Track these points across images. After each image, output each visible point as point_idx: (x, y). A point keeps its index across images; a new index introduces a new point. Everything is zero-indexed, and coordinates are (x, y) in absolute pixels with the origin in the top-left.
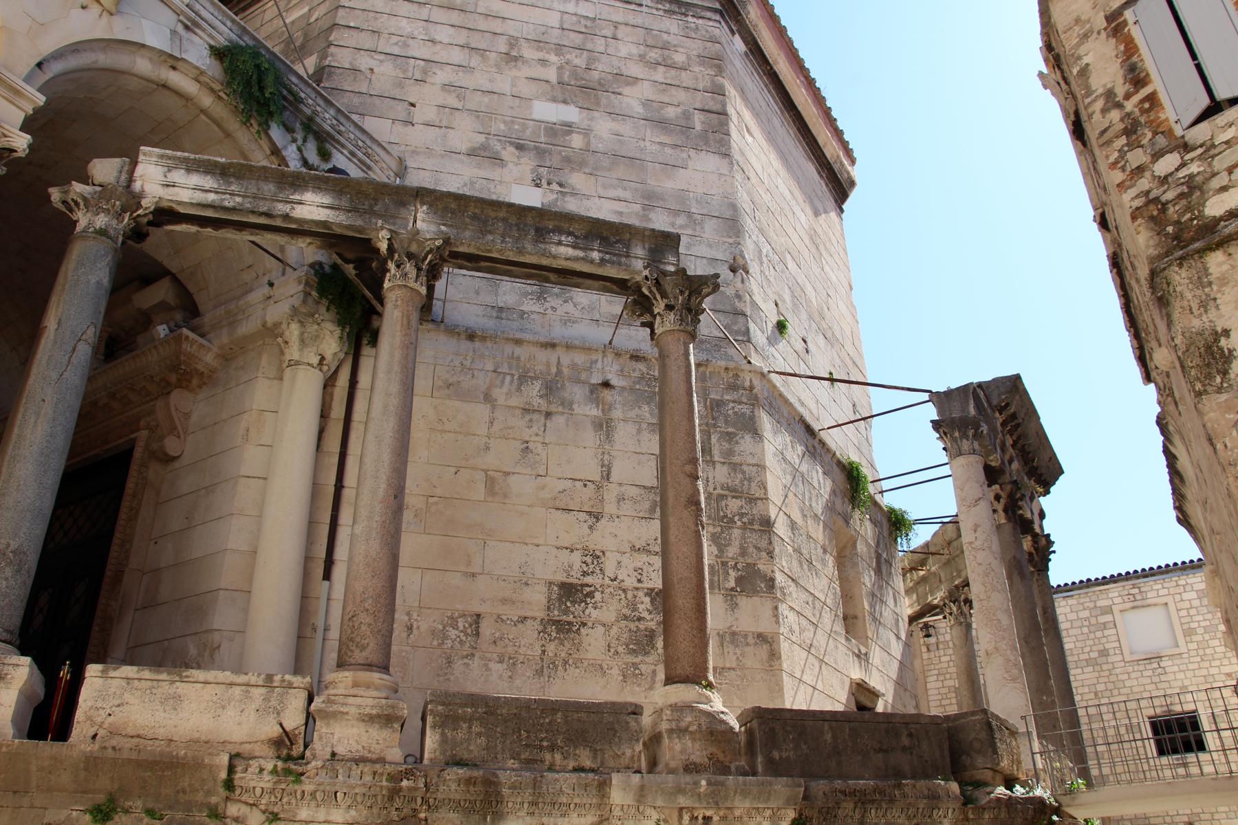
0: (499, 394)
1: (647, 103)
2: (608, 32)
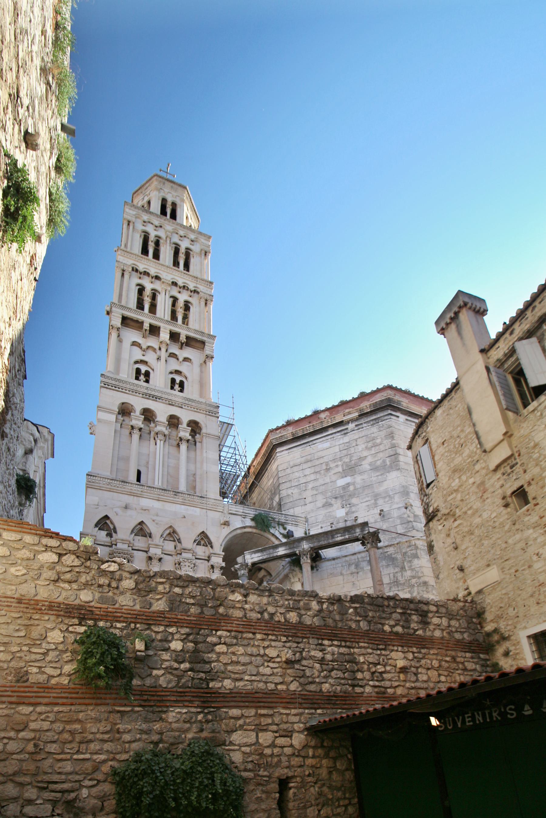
0: (344, 572)
1: (370, 464)
2: (354, 444)
